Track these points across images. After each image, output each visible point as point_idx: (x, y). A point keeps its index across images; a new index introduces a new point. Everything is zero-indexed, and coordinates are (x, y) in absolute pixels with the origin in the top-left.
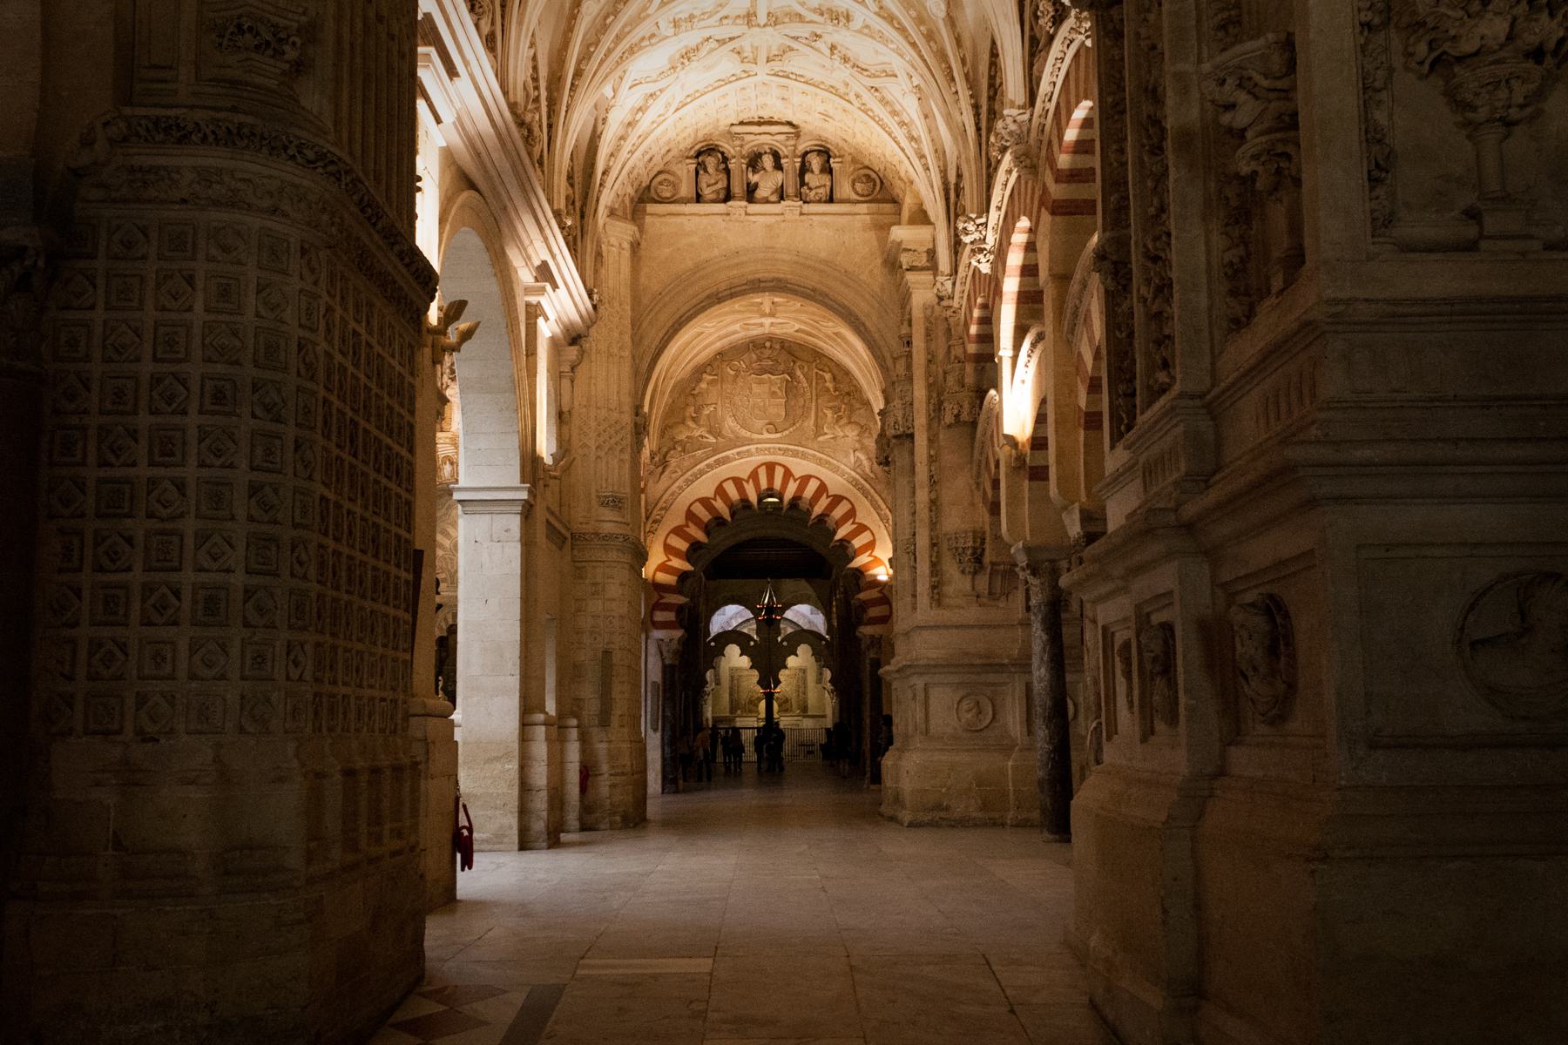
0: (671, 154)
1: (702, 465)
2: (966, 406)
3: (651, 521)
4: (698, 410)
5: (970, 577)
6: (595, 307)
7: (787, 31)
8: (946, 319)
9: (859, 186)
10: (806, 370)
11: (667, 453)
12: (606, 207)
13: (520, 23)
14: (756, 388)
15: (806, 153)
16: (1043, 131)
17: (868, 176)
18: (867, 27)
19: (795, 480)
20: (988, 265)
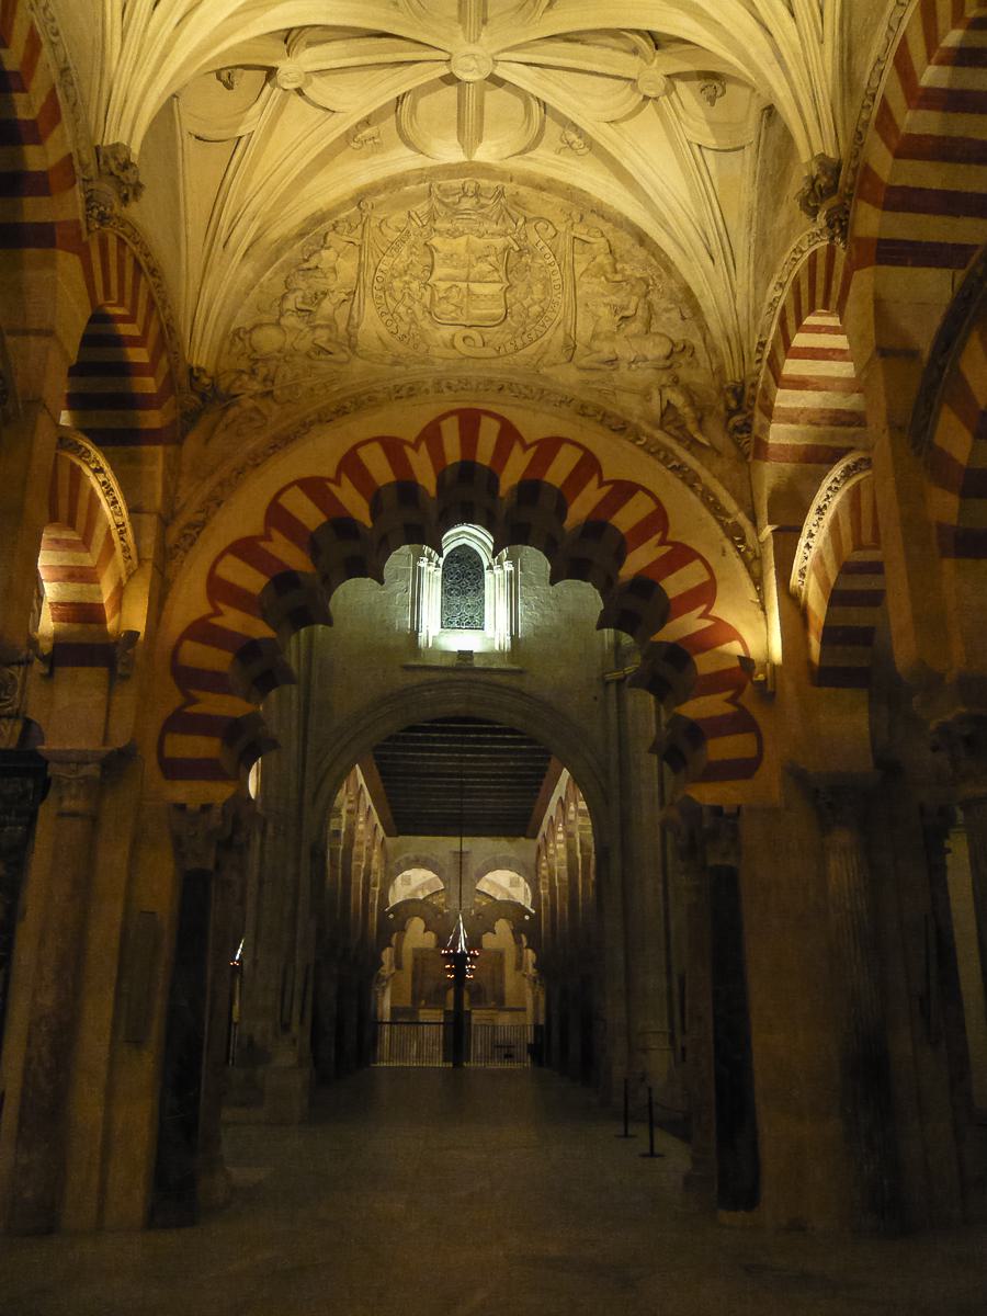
19: (526, 447)
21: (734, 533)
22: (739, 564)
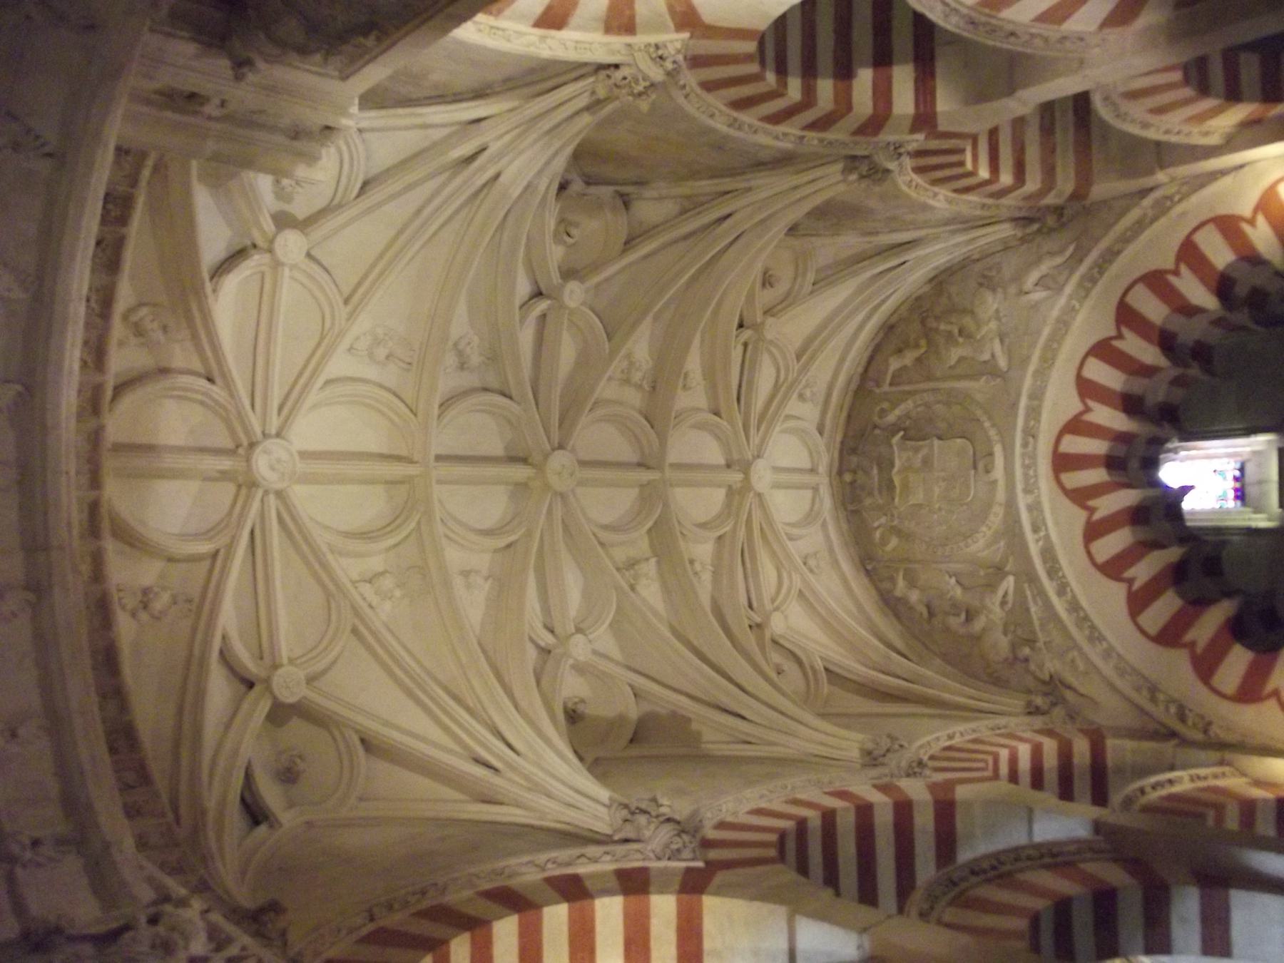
1: (1059, 606)
3: (1178, 727)
4: (955, 607)
10: (885, 405)
11: (1036, 678)
14: (918, 497)
21: (1162, 208)
22: (1194, 199)
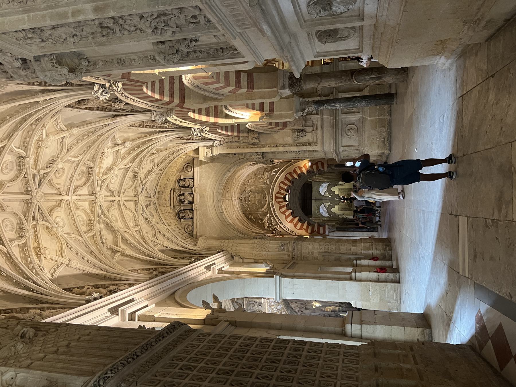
0: (179, 227)
1: (276, 218)
2: (253, 136)
4: (259, 219)
5: (307, 134)
6: (223, 251)
7: (140, 192)
8: (227, 142)
9: (189, 170)
12: (193, 247)
13: (126, 275)
15: (179, 186)
16: (158, 107)
17: (186, 168)
18: (138, 167)
20: (207, 127)
